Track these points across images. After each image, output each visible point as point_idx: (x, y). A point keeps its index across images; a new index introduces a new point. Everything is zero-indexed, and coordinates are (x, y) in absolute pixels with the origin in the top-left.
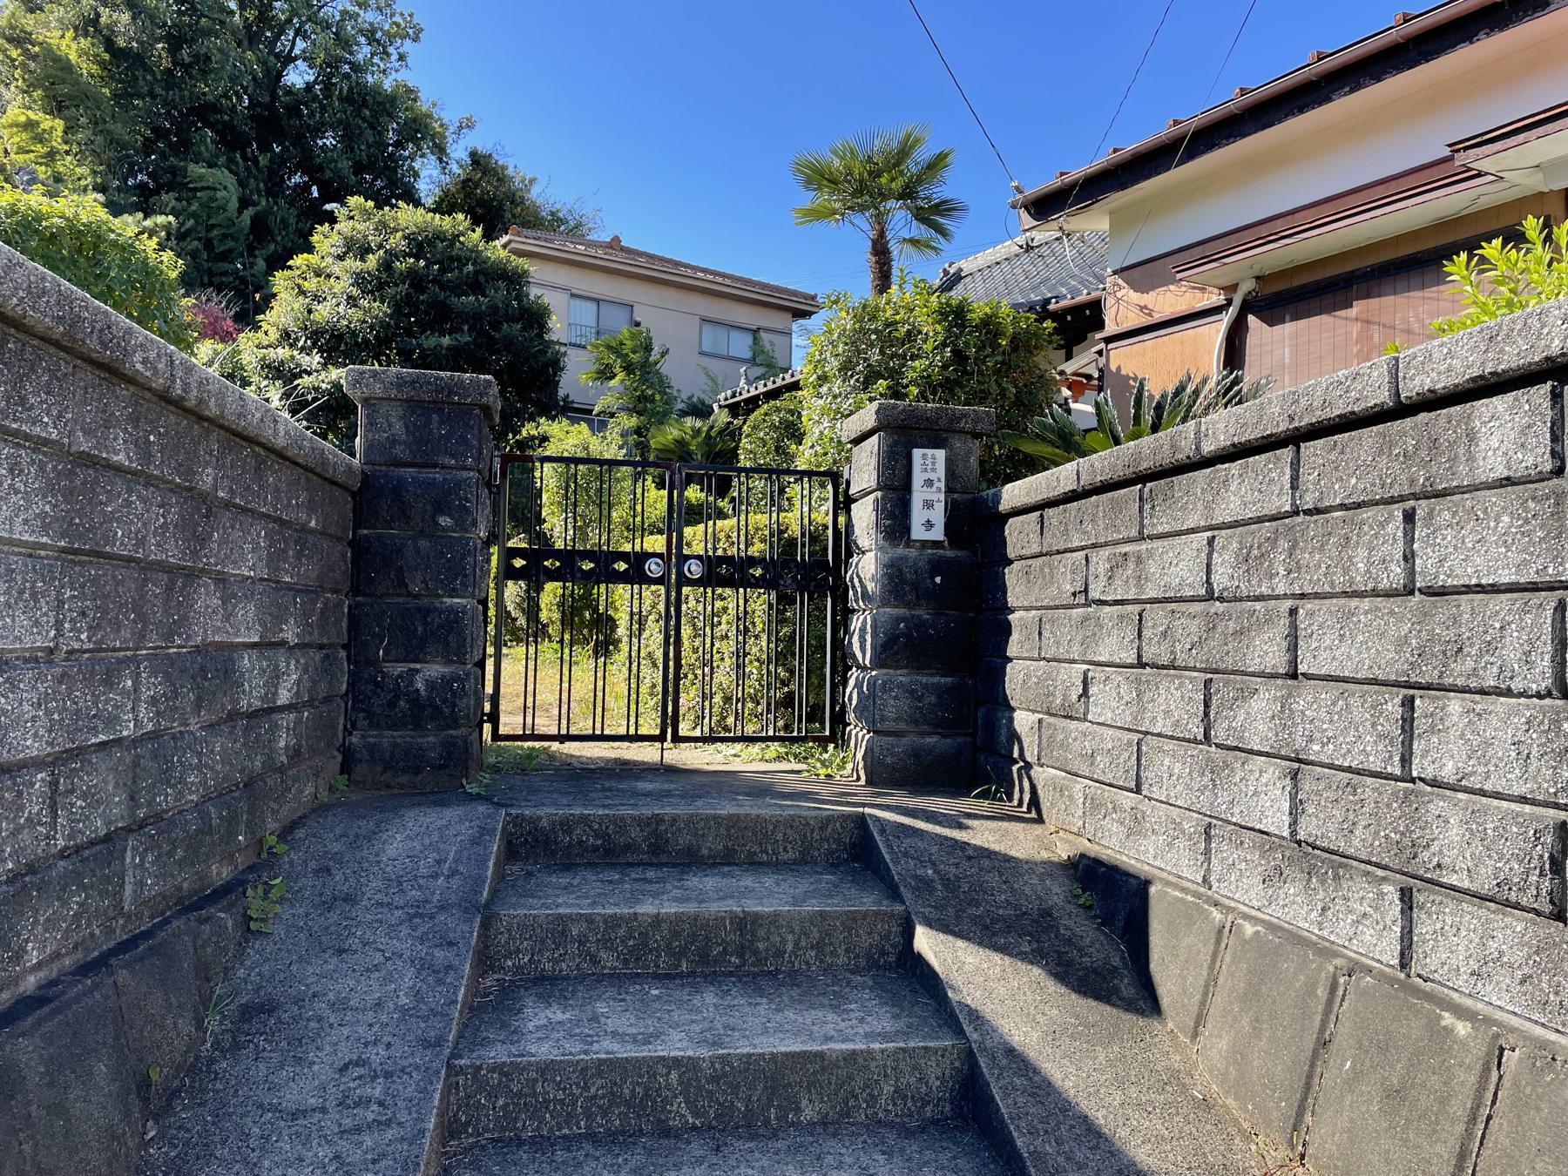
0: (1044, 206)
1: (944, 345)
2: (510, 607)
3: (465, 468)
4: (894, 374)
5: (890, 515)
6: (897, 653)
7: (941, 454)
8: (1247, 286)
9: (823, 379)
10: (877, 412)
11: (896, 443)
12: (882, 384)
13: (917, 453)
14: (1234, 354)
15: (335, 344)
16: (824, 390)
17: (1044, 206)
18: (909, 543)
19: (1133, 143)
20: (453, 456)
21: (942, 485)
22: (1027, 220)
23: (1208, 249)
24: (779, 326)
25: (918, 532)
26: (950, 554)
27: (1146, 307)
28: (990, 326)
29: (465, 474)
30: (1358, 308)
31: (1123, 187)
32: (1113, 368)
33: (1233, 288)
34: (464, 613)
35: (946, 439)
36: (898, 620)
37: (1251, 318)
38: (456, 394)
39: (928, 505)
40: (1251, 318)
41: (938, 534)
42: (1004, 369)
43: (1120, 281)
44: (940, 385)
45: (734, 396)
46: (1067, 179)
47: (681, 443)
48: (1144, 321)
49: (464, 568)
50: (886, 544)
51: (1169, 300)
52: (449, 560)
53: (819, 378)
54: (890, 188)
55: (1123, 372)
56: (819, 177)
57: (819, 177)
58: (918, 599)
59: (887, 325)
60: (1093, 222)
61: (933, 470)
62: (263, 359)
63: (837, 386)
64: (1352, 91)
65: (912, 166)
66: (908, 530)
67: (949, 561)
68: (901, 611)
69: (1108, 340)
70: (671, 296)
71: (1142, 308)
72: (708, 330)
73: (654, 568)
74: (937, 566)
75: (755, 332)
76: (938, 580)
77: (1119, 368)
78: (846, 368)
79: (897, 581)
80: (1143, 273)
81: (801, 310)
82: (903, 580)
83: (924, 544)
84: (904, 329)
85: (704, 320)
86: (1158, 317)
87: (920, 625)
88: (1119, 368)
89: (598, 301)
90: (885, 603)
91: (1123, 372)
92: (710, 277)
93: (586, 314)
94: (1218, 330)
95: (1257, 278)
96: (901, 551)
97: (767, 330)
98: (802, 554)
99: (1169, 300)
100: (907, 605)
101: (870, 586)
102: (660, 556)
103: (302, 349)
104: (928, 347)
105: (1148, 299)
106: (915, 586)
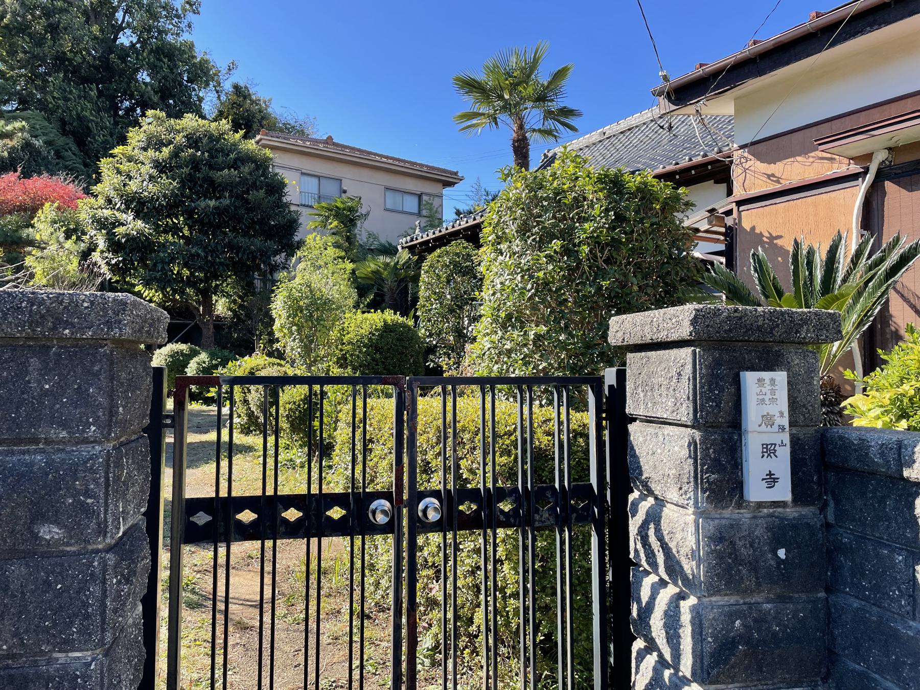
0: (683, 93)
1: (607, 210)
2: (253, 409)
3: (86, 441)
4: (567, 234)
5: (716, 466)
6: (732, 667)
7: (781, 377)
8: (881, 156)
9: (499, 240)
10: (694, 322)
11: (717, 363)
12: (556, 244)
13: (750, 379)
14: (871, 216)
15: (139, 206)
16: (503, 246)
17: (683, 93)
18: (741, 502)
19: (772, 36)
20: (63, 425)
21: (785, 422)
22: (664, 105)
23: (862, 119)
25: (756, 491)
26: (792, 512)
27: (773, 175)
28: (644, 194)
29: (85, 450)
31: (761, 73)
32: (746, 225)
33: (868, 157)
34: (86, 677)
35: (779, 355)
36: (732, 616)
37: (888, 185)
38: (67, 324)
39: (769, 450)
40: (888, 185)
41: (783, 492)
42: (656, 227)
43: (746, 154)
44: (607, 245)
45: (412, 240)
46: (709, 69)
47: (376, 272)
48: (777, 187)
49: (85, 605)
50: (711, 507)
51: (795, 170)
52: (59, 594)
53: (498, 237)
54: (520, 97)
55: (757, 231)
56: (471, 86)
57: (471, 86)
58: (758, 584)
59: (557, 194)
60: (720, 107)
61: (773, 400)
62: (94, 216)
65: (542, 77)
66: (738, 487)
67: (796, 525)
68: (733, 599)
69: (740, 203)
70: (366, 174)
71: (769, 176)
72: (389, 194)
73: (380, 511)
74: (782, 532)
76: (782, 553)
77: (753, 228)
78: (524, 230)
79: (729, 559)
80: (768, 147)
81: (448, 180)
82: (738, 561)
83: (760, 505)
84: (571, 196)
85: (387, 189)
86: (786, 184)
87: (761, 620)
88: (753, 228)
89: (319, 177)
90: (712, 590)
92: (391, 161)
93: (311, 185)
94: (859, 192)
96: (729, 513)
97: (427, 194)
98: (561, 479)
99: (795, 170)
100: (738, 591)
101: (689, 567)
102: (386, 495)
103: (118, 209)
104: (597, 210)
105: (776, 168)
106: (754, 568)
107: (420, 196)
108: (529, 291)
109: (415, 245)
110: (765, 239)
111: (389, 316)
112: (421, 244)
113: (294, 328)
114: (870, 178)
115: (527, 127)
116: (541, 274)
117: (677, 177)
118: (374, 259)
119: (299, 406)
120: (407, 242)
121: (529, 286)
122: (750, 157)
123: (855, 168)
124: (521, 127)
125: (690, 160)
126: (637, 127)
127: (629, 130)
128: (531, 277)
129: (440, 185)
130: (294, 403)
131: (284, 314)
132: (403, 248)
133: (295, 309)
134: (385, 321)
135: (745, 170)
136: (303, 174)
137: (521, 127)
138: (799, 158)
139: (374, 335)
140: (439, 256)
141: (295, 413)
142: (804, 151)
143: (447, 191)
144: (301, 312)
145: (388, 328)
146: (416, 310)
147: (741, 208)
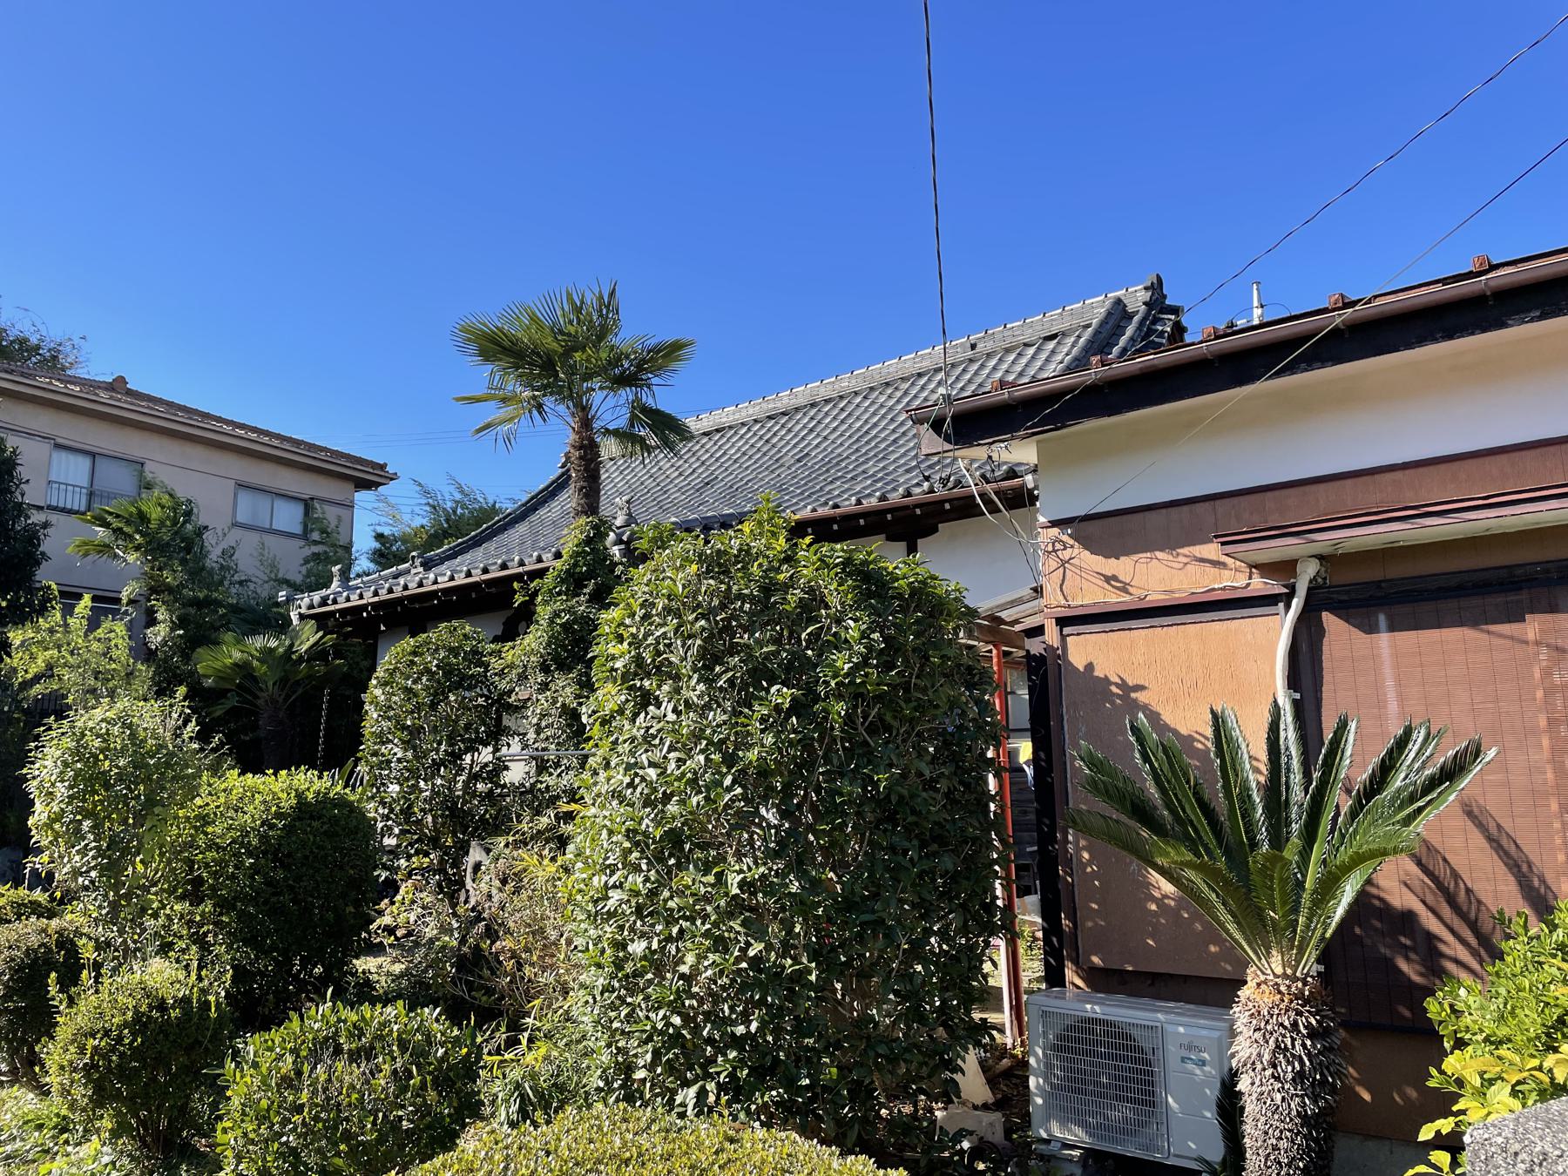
12: (781, 695)
14: (1304, 667)
24: (338, 497)
27: (1115, 578)
30: (1532, 626)
33: (1284, 569)
37: (1328, 619)
40: (1328, 619)
43: (1065, 538)
45: (324, 602)
47: (243, 668)
55: (1098, 673)
63: (695, 690)
64: (1540, 318)
70: (196, 454)
72: (245, 499)
75: (308, 505)
77: (1090, 667)
78: (709, 660)
81: (368, 477)
84: (795, 596)
85: (241, 485)
88: (1090, 667)
89: (93, 455)
91: (1098, 673)
92: (276, 442)
93: (74, 470)
94: (1280, 628)
95: (1321, 558)
97: (323, 501)
99: (1157, 575)
105: (1121, 567)
107: (308, 505)
108: (729, 789)
109: (332, 613)
110: (1114, 689)
111: (308, 782)
112: (343, 612)
113: (87, 824)
114: (1297, 603)
115: (596, 425)
116: (753, 755)
117: (835, 527)
118: (238, 642)
119: (119, 1039)
120: (311, 607)
121: (728, 781)
122: (1071, 542)
123: (1260, 585)
124: (586, 424)
125: (859, 502)
126: (730, 427)
127: (718, 431)
128: (730, 760)
129: (351, 486)
130: (107, 1033)
131: (61, 790)
132: (302, 617)
133: (87, 776)
134: (300, 795)
135: (1064, 563)
136: (58, 446)
137: (586, 424)
138: (1159, 554)
139: (272, 827)
140: (415, 653)
141: (106, 1057)
142: (1170, 543)
143: (362, 497)
144: (107, 786)
145: (305, 811)
146: (358, 760)
147: (1066, 630)
